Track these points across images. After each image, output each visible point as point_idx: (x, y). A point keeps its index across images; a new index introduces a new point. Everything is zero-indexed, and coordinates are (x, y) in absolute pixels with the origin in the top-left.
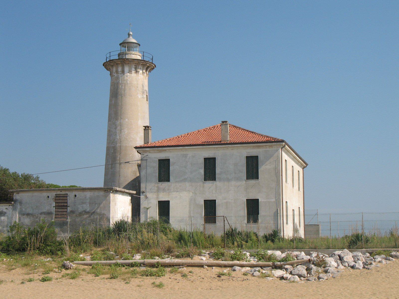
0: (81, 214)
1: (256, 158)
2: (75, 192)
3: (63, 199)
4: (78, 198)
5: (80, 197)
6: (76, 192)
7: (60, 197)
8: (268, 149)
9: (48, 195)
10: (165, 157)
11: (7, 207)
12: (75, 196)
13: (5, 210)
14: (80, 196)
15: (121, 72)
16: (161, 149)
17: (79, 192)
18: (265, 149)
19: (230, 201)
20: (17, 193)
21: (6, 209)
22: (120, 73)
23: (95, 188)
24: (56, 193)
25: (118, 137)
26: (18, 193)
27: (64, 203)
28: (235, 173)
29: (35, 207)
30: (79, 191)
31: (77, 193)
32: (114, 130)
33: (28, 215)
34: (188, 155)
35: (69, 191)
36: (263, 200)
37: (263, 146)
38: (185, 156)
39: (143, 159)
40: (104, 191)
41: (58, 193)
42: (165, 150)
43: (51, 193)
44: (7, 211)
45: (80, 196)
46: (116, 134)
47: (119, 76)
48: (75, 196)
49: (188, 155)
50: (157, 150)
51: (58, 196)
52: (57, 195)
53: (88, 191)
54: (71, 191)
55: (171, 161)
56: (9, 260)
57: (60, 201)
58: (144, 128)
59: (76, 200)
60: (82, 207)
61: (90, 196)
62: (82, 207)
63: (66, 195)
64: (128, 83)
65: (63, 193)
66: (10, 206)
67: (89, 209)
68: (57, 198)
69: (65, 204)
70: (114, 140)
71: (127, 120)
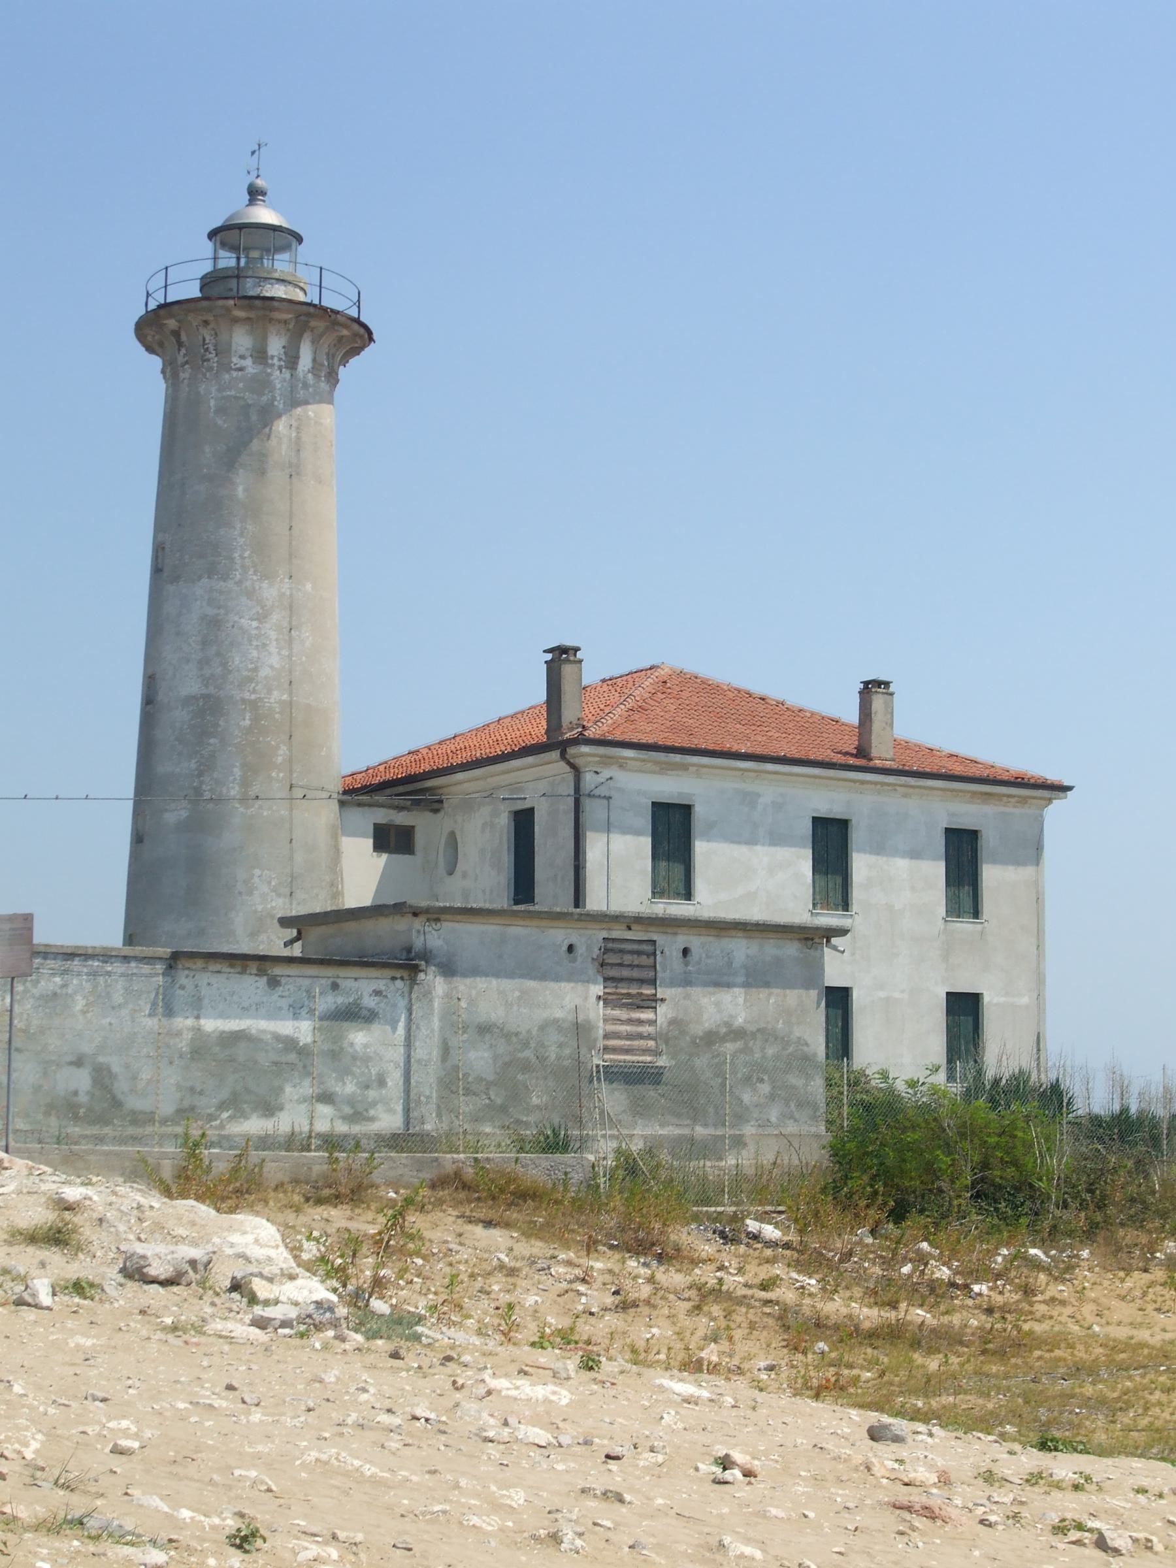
0: (711, 1038)
1: (685, 811)
2: (685, 937)
3: (638, 966)
4: (699, 963)
5: (709, 961)
6: (692, 938)
7: (621, 951)
8: (1009, 810)
9: (573, 939)
10: (680, 794)
11: (381, 985)
12: (686, 952)
13: (369, 1002)
14: (708, 957)
15: (280, 359)
16: (661, 756)
17: (703, 939)
18: (1002, 809)
19: (897, 995)
20: (428, 920)
21: (377, 993)
22: (275, 361)
23: (784, 926)
24: (605, 934)
25: (274, 660)
26: (437, 920)
27: (642, 982)
28: (913, 889)
29: (517, 994)
30: (703, 931)
31: (695, 942)
32: (255, 624)
33: (484, 1029)
34: (759, 795)
35: (662, 929)
36: (995, 1000)
37: (1000, 796)
38: (750, 799)
39: (597, 792)
40: (799, 939)
41: (615, 934)
42: (685, 767)
43: (582, 931)
44: (382, 1005)
45: (708, 957)
46: (264, 645)
47: (270, 375)
48: (686, 952)
49: (759, 795)
50: (656, 763)
51: (612, 950)
52: (610, 945)
53: (740, 934)
54: (669, 930)
55: (699, 811)
56: (906, 1269)
57: (626, 973)
58: (549, 656)
59: (690, 972)
60: (717, 1004)
61: (748, 956)
62: (717, 1004)
63: (647, 948)
64: (308, 416)
65: (636, 934)
66: (394, 979)
67: (743, 1015)
68: (612, 959)
69: (647, 991)
70: (256, 670)
71: (309, 586)
